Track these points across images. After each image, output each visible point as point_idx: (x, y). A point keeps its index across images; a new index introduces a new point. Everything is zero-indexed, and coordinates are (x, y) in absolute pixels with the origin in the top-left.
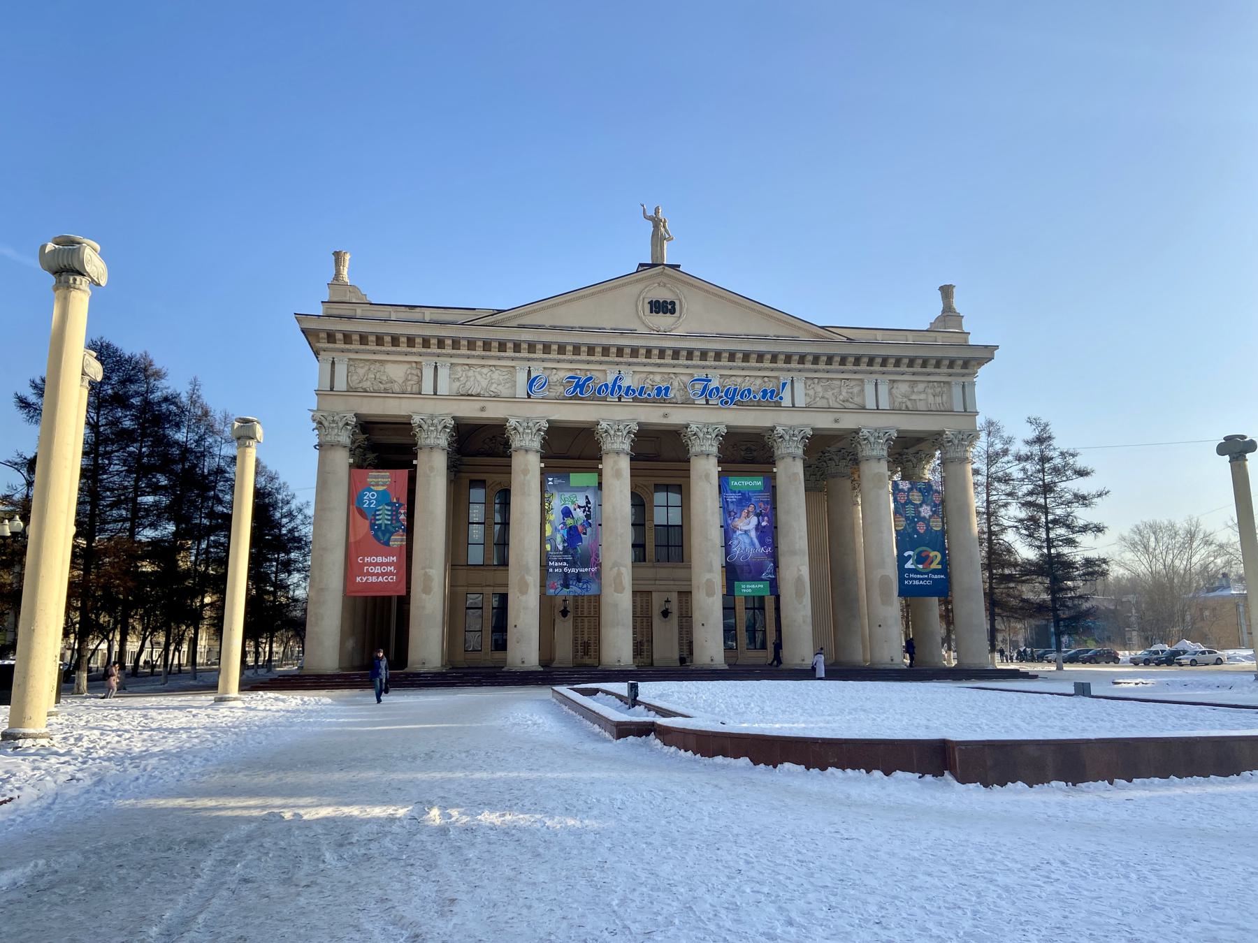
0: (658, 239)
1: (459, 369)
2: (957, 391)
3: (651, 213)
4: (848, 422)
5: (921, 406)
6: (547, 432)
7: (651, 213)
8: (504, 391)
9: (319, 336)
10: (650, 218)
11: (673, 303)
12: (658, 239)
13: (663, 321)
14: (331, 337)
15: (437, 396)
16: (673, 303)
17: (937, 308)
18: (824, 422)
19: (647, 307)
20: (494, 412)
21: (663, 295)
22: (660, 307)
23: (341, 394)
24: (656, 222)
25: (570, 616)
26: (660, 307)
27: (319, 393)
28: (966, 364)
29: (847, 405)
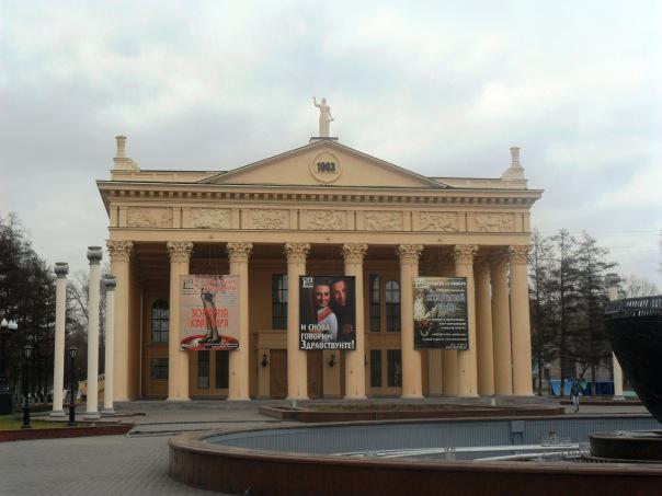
0: (325, 121)
1: (196, 211)
2: (519, 219)
3: (319, 102)
4: (447, 241)
5: (496, 230)
6: (253, 250)
7: (319, 102)
8: (225, 225)
9: (111, 194)
10: (319, 106)
11: (333, 164)
12: (325, 121)
13: (327, 178)
14: (117, 193)
15: (182, 229)
16: (333, 164)
17: (508, 163)
18: (432, 241)
19: (317, 167)
20: (218, 238)
21: (326, 159)
22: (326, 168)
23: (123, 229)
24: (325, 110)
25: (268, 366)
26: (326, 168)
27: (110, 229)
28: (524, 201)
29: (448, 230)
